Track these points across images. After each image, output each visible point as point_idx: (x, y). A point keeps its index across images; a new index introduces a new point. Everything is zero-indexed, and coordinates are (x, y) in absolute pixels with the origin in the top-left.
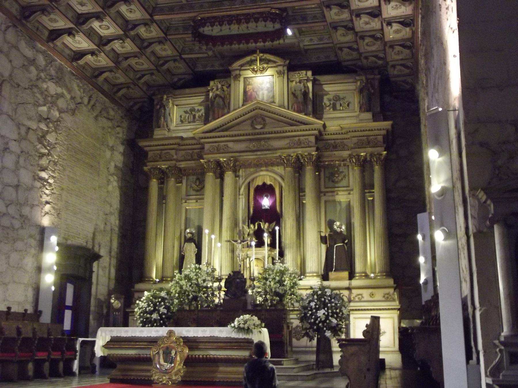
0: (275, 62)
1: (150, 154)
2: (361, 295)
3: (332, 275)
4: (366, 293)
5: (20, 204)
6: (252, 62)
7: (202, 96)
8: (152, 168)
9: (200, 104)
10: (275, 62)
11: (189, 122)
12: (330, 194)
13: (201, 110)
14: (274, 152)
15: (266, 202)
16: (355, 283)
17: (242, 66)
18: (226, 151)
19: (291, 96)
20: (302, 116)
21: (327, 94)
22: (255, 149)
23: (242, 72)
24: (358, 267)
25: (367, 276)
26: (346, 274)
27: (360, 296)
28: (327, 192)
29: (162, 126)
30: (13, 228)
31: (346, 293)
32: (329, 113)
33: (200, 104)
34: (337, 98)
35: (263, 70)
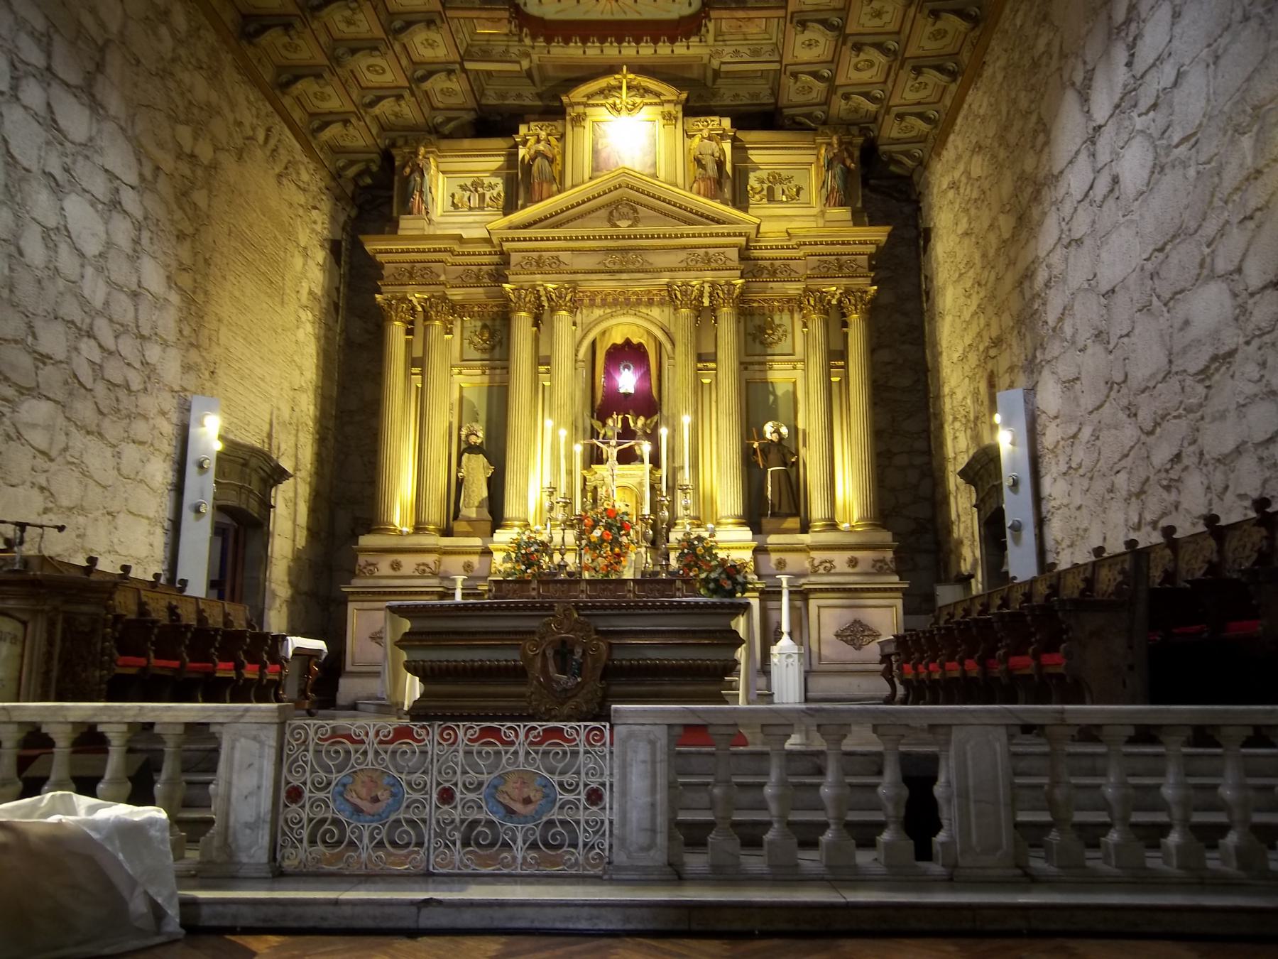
0: (658, 95)
2: (830, 562)
5: (142, 337)
7: (499, 155)
8: (393, 298)
9: (495, 173)
10: (658, 95)
11: (471, 209)
12: (757, 367)
13: (496, 185)
14: (656, 275)
15: (627, 381)
17: (589, 96)
18: (555, 266)
19: (692, 166)
20: (716, 207)
21: (756, 168)
22: (616, 267)
23: (589, 110)
27: (828, 565)
28: (752, 364)
29: (415, 210)
30: (128, 388)
33: (495, 173)
34: (776, 179)
35: (632, 108)
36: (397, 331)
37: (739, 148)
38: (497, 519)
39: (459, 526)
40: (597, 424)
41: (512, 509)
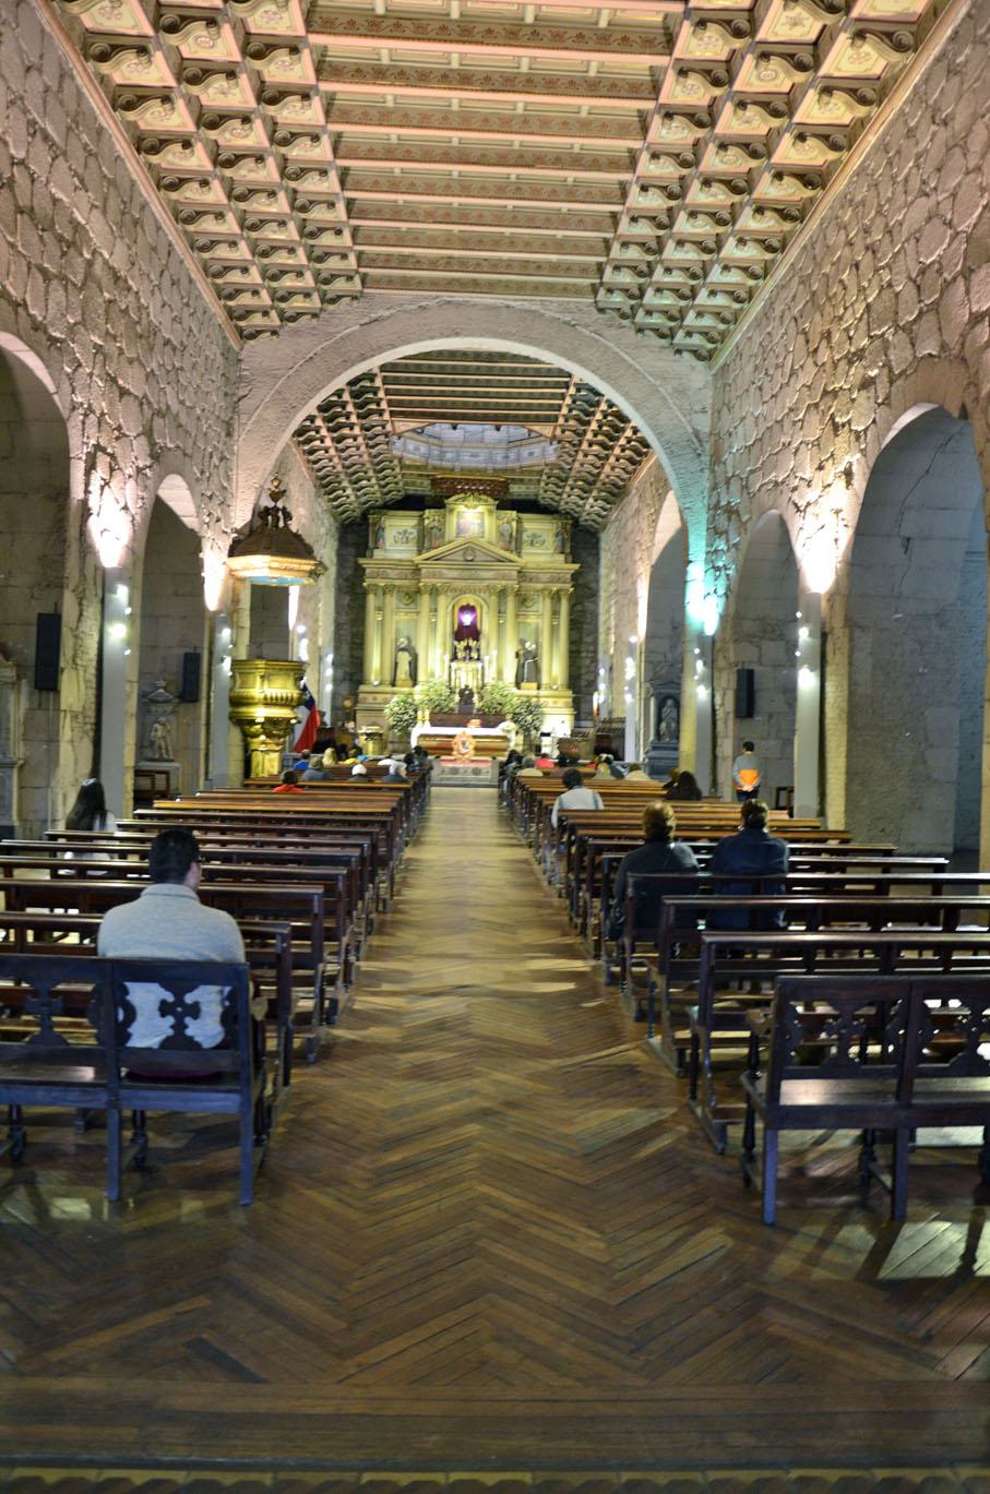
1: (368, 571)
3: (523, 685)
4: (550, 701)
6: (464, 499)
9: (413, 527)
16: (542, 692)
20: (507, 555)
24: (545, 679)
25: (551, 688)
26: (535, 685)
31: (534, 700)
32: (526, 549)
33: (413, 527)
34: (534, 536)
35: (476, 507)
36: (372, 601)
37: (519, 521)
38: (413, 677)
39: (398, 683)
40: (456, 643)
41: (421, 677)
